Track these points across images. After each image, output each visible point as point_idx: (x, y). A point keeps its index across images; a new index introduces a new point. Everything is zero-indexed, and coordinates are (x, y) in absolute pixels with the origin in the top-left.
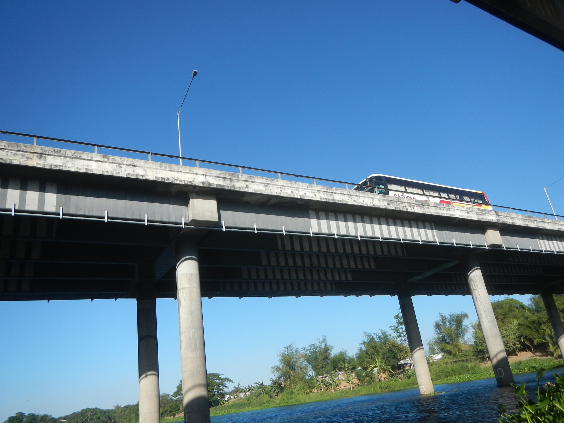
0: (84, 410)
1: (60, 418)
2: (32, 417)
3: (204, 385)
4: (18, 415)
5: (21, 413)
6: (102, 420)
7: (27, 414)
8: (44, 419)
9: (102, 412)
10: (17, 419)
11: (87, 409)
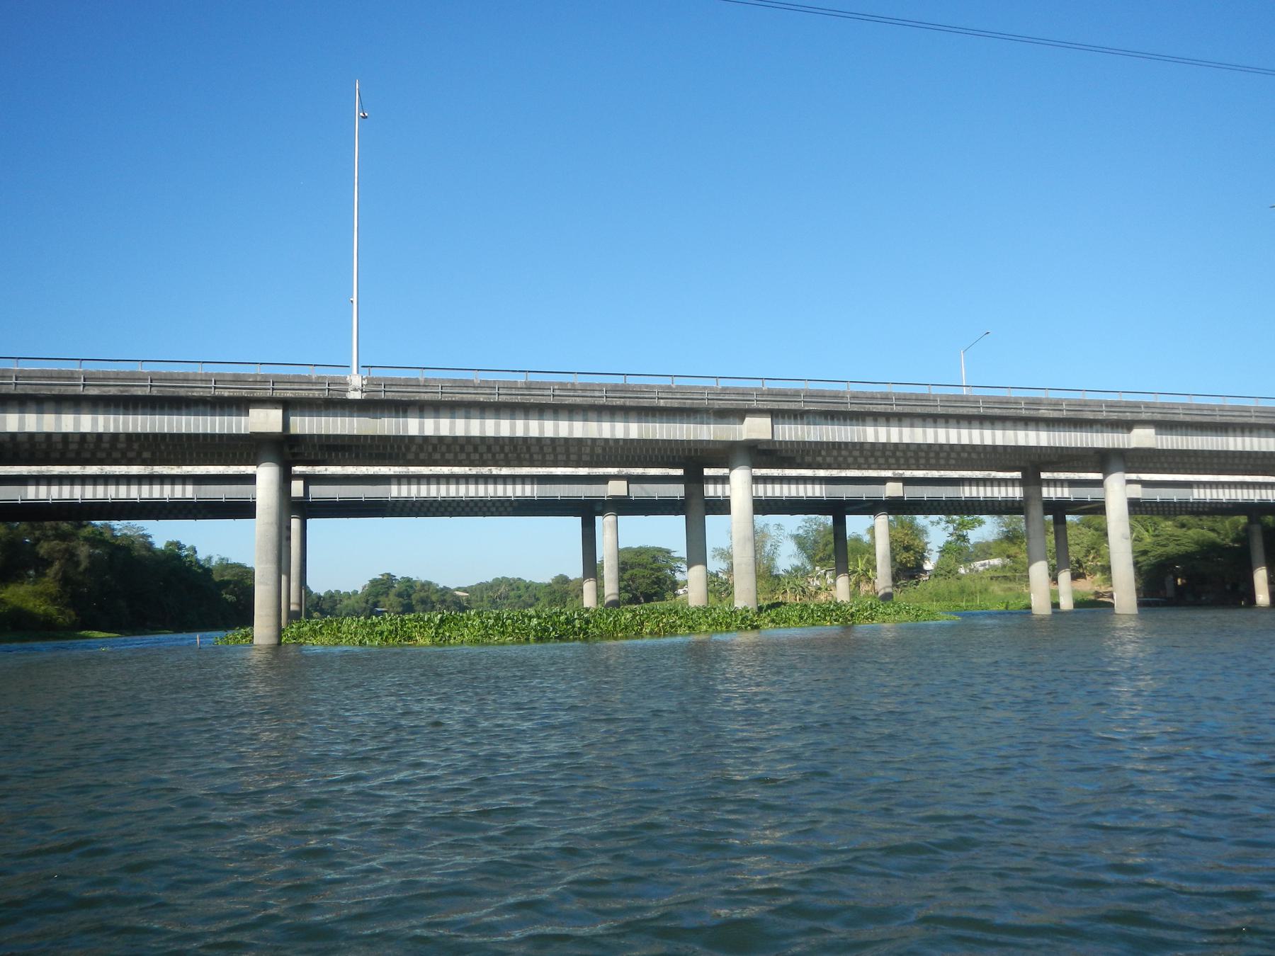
0: (497, 579)
1: (459, 589)
2: (408, 584)
3: (297, 604)
4: (385, 578)
5: (389, 574)
6: (523, 601)
7: (398, 577)
8: (426, 588)
9: (528, 586)
10: (383, 584)
11: (503, 578)
